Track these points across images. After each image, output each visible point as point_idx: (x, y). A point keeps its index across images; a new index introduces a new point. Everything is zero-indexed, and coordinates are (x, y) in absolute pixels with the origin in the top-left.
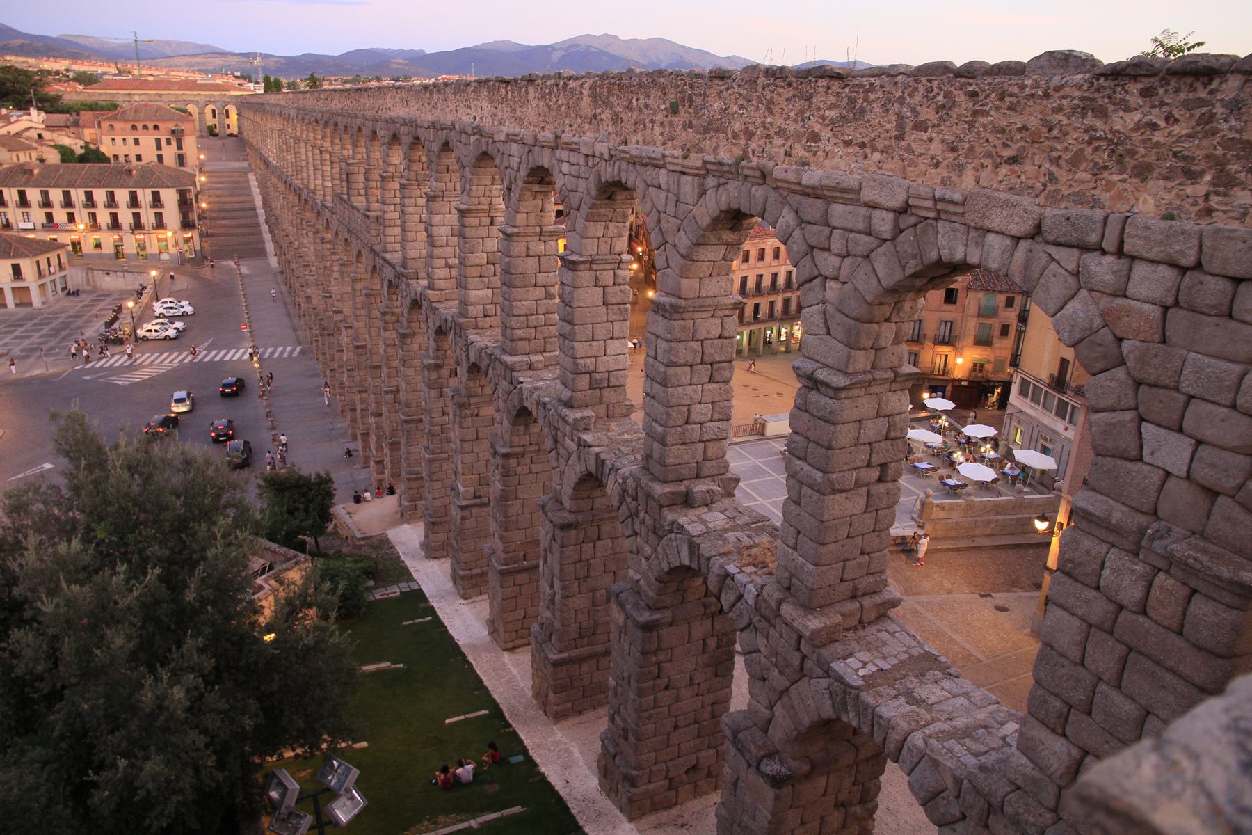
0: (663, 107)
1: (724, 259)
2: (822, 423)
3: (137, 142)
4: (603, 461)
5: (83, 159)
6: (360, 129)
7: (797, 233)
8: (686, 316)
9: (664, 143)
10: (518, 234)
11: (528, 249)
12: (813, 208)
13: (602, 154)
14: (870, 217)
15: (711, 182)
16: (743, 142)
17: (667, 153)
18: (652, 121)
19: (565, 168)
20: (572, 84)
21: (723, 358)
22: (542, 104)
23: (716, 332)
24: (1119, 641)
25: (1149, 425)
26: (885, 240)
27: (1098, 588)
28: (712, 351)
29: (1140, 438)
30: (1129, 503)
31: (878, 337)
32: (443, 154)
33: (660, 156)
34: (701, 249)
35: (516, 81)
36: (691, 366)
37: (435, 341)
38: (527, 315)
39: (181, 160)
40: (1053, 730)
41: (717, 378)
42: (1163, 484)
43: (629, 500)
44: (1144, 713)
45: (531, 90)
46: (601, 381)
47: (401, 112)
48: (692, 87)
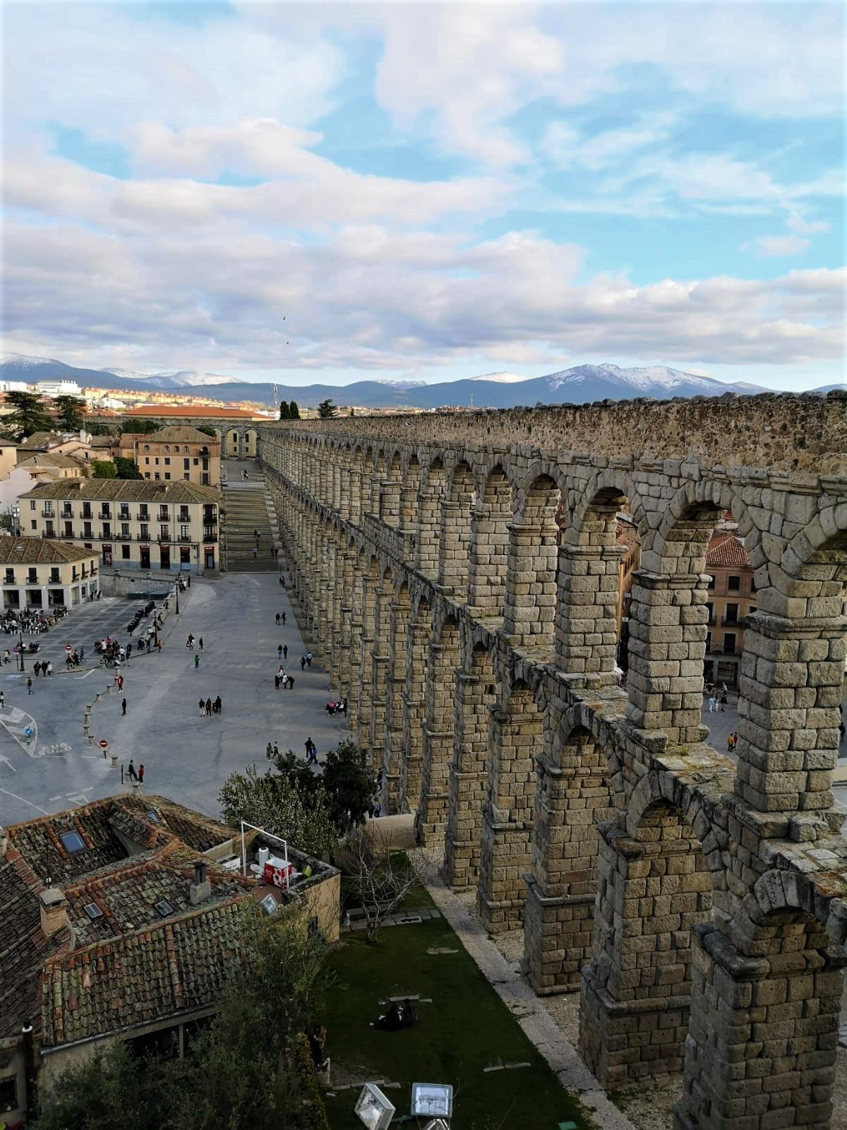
0: (768, 429)
3: (167, 461)
4: (684, 786)
5: (121, 475)
6: (397, 453)
9: (770, 464)
10: (580, 553)
11: (589, 568)
15: (824, 500)
17: (774, 473)
18: (755, 443)
19: (643, 489)
20: (655, 409)
21: (831, 682)
22: (616, 428)
32: (493, 477)
33: (765, 475)
34: (811, 569)
35: (586, 406)
36: (796, 688)
37: (473, 656)
38: (584, 633)
39: (206, 479)
41: (824, 702)
43: (716, 829)
45: (605, 415)
47: (448, 436)
48: (805, 408)
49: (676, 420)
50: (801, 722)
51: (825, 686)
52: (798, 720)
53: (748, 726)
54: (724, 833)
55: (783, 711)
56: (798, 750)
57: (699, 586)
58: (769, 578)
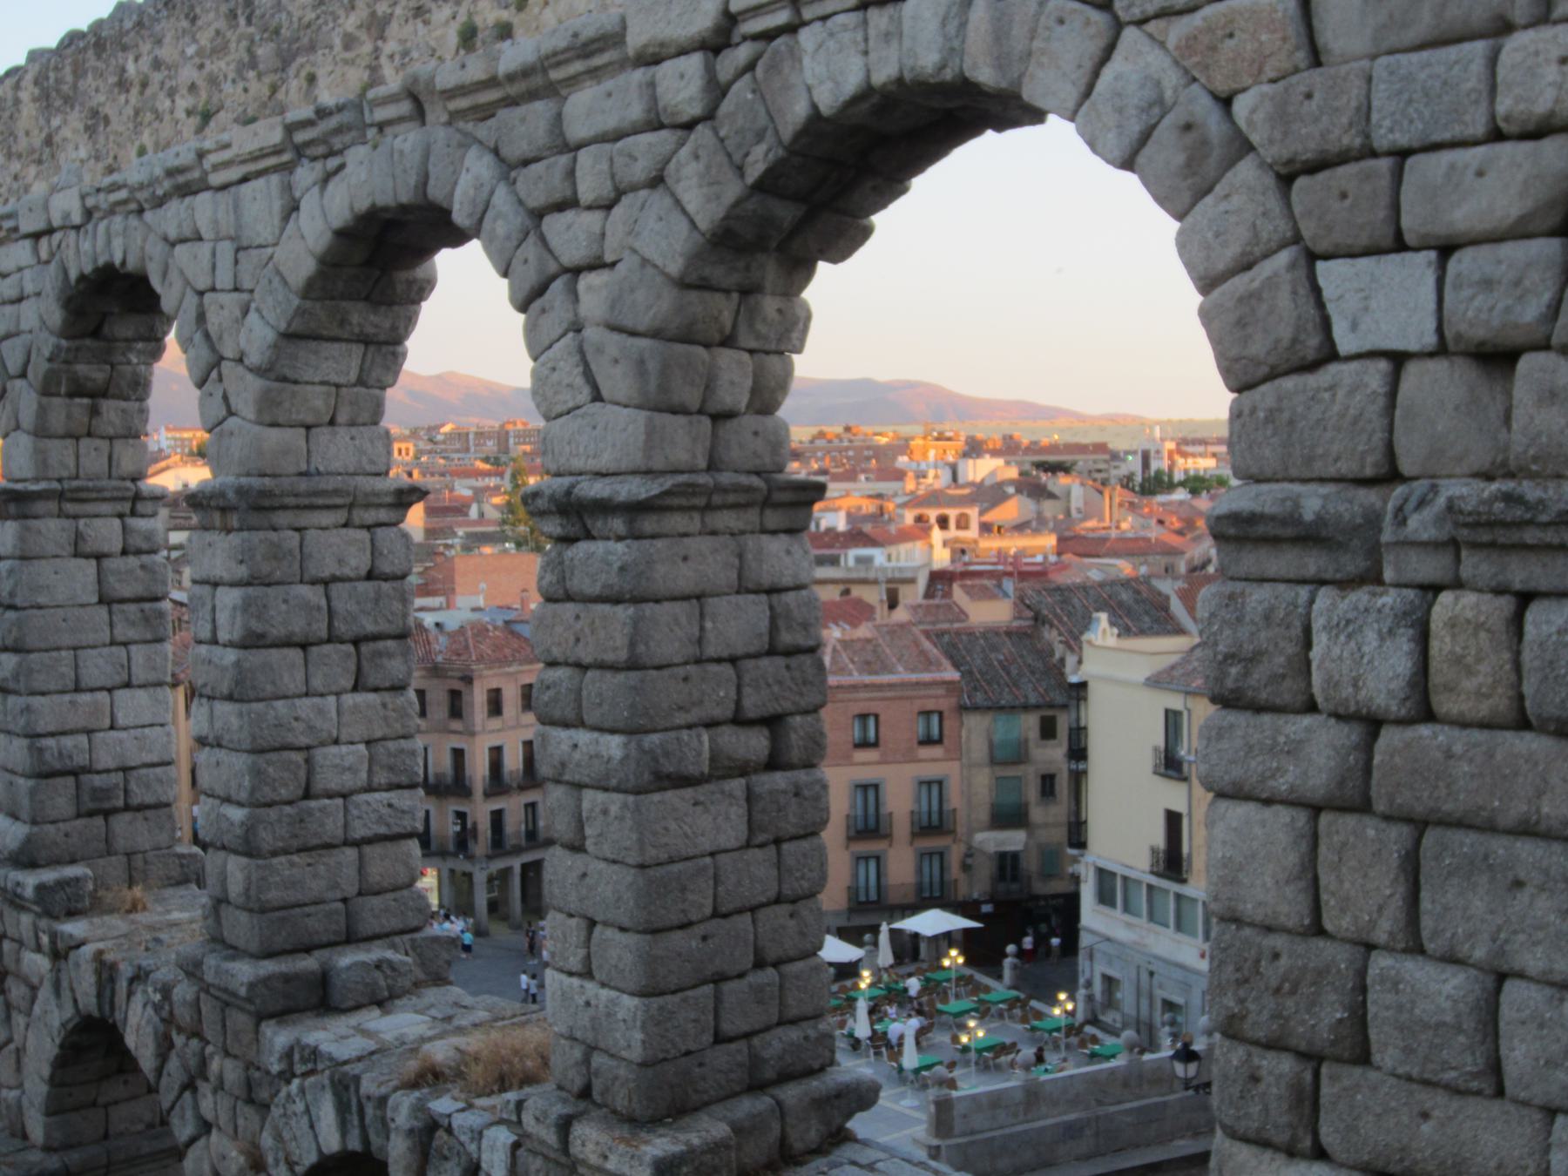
0: (191, 51)
1: (361, 382)
2: (606, 608)
7: (501, 197)
8: (282, 518)
12: (526, 126)
13: (67, 215)
14: (652, 85)
15: (305, 174)
16: (367, 48)
18: (172, 93)
21: (383, 627)
23: (358, 561)
24: (1388, 818)
25: (1332, 264)
26: (690, 126)
27: (1311, 707)
28: (352, 607)
29: (1320, 304)
30: (1332, 471)
31: (709, 387)
36: (304, 646)
40: (1291, 1153)
41: (373, 678)
42: (1392, 394)
43: (179, 1040)
44: (1490, 982)
46: (106, 793)
49: (35, 100)
50: (328, 726)
51: (376, 638)
52: (318, 723)
53: (213, 760)
54: (194, 1043)
55: (279, 704)
56: (330, 795)
57: (140, 507)
58: (225, 398)
